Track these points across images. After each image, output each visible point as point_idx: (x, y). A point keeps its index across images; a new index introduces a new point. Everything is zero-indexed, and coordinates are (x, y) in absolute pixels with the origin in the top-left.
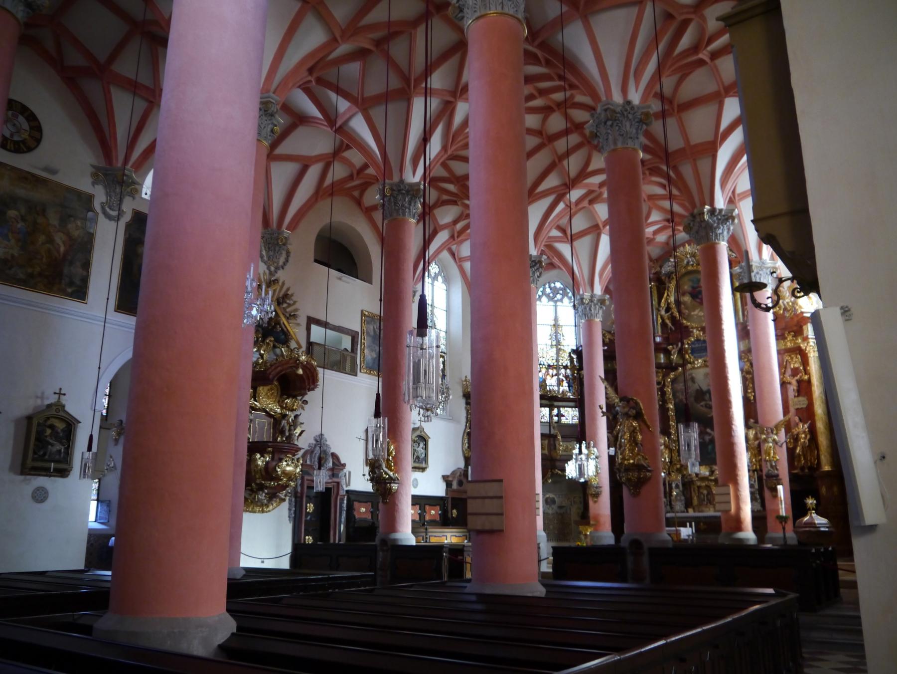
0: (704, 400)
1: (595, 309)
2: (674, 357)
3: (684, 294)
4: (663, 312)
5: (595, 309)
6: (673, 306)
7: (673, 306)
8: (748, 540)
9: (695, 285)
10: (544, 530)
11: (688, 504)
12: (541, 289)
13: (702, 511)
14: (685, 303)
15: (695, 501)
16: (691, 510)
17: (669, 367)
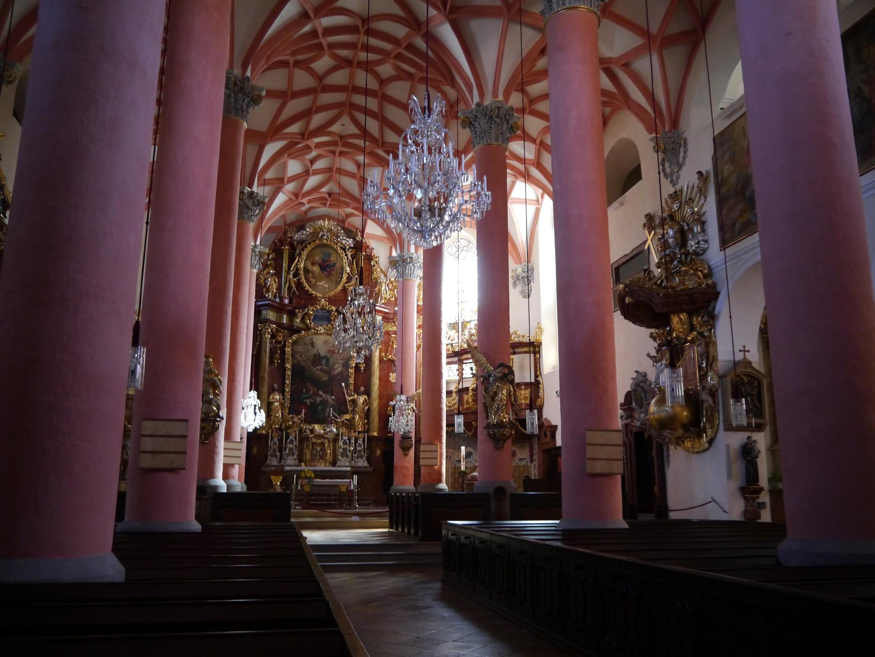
3: (313, 264)
4: (291, 276)
6: (302, 272)
7: (302, 272)
11: (301, 459)
13: (314, 466)
14: (313, 272)
15: (308, 457)
16: (303, 464)
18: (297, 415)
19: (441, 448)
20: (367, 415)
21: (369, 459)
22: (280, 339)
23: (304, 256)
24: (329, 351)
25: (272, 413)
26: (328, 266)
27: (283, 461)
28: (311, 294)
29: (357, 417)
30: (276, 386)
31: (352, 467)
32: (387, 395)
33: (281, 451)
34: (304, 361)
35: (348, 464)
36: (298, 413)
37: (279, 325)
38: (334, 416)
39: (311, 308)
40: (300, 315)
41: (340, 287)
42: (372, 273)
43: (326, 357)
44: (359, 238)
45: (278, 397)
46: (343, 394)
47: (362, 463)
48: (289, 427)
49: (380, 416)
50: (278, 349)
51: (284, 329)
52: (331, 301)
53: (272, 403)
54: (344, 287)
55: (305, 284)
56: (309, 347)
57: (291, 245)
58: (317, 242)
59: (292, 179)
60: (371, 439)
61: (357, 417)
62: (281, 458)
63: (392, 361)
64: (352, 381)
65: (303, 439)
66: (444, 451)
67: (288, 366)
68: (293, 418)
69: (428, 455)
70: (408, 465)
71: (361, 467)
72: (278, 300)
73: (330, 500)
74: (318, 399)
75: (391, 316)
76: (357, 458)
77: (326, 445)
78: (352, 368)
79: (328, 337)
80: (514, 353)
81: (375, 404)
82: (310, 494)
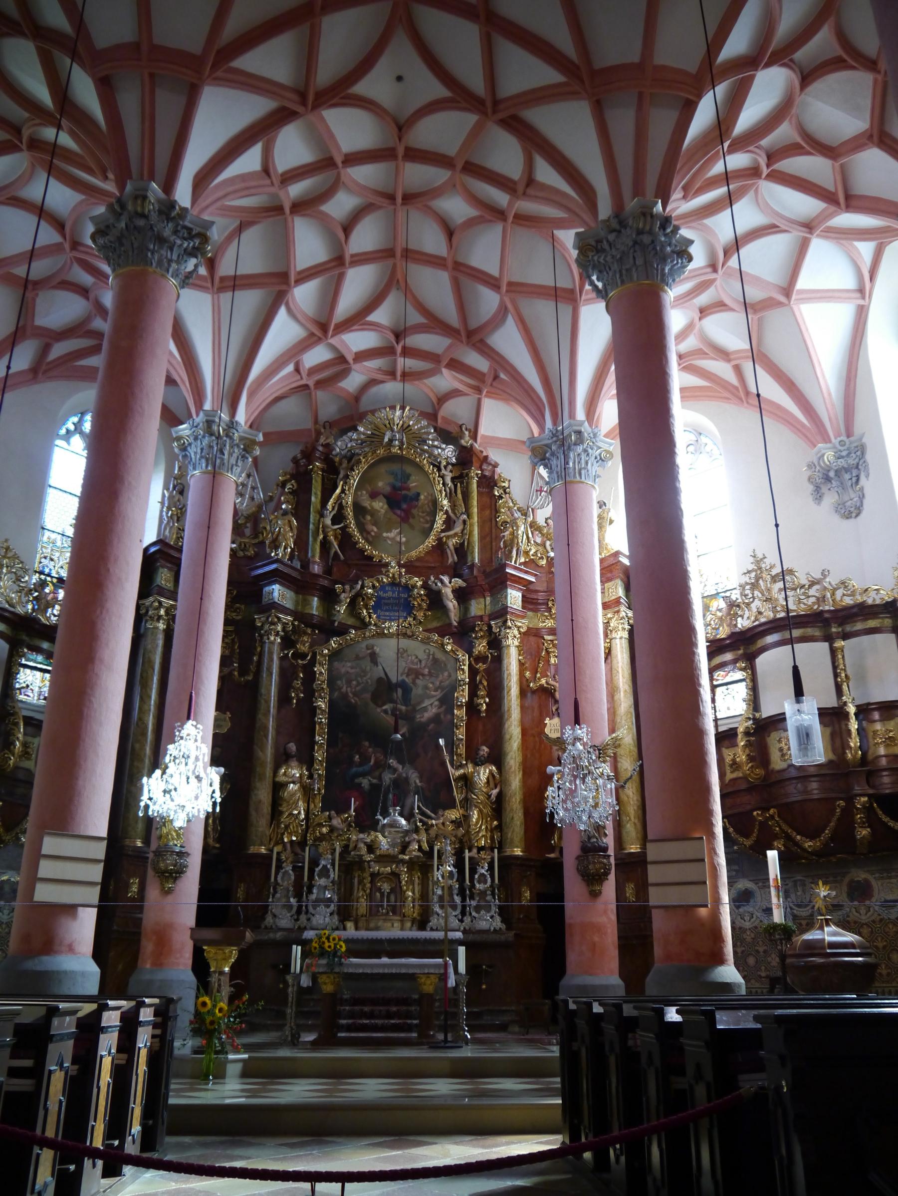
0: (392, 701)
1: (231, 454)
3: (373, 496)
4: (328, 521)
5: (231, 454)
6: (350, 513)
7: (350, 513)
8: (606, 987)
9: (398, 484)
10: (98, 955)
11: (344, 914)
12: (75, 419)
13: (377, 928)
14: (373, 513)
16: (350, 925)
17: (328, 629)
18: (339, 813)
19: (713, 851)
20: (498, 807)
21: (503, 912)
22: (303, 648)
23: (354, 481)
25: (283, 808)
26: (405, 498)
27: (303, 917)
28: (370, 558)
29: (475, 815)
30: (292, 747)
31: (464, 932)
32: (542, 755)
33: (298, 895)
34: (355, 694)
35: (455, 923)
38: (422, 813)
39: (368, 582)
40: (345, 598)
41: (431, 541)
42: (497, 511)
43: (402, 685)
44: (466, 441)
47: (489, 921)
48: (322, 838)
49: (526, 813)
52: (411, 568)
53: (284, 785)
54: (439, 540)
56: (367, 664)
57: (328, 459)
58: (381, 452)
59: (306, 276)
60: (507, 863)
61: (475, 815)
62: (299, 912)
63: (547, 693)
65: (350, 866)
66: (722, 860)
67: (322, 704)
68: (330, 818)
70: (603, 919)
71: (487, 931)
73: (409, 1015)
74: (388, 777)
75: (541, 596)
76: (478, 909)
77: (404, 877)
78: (460, 707)
79: (404, 643)
80: (846, 636)
81: (515, 782)
82: (334, 999)
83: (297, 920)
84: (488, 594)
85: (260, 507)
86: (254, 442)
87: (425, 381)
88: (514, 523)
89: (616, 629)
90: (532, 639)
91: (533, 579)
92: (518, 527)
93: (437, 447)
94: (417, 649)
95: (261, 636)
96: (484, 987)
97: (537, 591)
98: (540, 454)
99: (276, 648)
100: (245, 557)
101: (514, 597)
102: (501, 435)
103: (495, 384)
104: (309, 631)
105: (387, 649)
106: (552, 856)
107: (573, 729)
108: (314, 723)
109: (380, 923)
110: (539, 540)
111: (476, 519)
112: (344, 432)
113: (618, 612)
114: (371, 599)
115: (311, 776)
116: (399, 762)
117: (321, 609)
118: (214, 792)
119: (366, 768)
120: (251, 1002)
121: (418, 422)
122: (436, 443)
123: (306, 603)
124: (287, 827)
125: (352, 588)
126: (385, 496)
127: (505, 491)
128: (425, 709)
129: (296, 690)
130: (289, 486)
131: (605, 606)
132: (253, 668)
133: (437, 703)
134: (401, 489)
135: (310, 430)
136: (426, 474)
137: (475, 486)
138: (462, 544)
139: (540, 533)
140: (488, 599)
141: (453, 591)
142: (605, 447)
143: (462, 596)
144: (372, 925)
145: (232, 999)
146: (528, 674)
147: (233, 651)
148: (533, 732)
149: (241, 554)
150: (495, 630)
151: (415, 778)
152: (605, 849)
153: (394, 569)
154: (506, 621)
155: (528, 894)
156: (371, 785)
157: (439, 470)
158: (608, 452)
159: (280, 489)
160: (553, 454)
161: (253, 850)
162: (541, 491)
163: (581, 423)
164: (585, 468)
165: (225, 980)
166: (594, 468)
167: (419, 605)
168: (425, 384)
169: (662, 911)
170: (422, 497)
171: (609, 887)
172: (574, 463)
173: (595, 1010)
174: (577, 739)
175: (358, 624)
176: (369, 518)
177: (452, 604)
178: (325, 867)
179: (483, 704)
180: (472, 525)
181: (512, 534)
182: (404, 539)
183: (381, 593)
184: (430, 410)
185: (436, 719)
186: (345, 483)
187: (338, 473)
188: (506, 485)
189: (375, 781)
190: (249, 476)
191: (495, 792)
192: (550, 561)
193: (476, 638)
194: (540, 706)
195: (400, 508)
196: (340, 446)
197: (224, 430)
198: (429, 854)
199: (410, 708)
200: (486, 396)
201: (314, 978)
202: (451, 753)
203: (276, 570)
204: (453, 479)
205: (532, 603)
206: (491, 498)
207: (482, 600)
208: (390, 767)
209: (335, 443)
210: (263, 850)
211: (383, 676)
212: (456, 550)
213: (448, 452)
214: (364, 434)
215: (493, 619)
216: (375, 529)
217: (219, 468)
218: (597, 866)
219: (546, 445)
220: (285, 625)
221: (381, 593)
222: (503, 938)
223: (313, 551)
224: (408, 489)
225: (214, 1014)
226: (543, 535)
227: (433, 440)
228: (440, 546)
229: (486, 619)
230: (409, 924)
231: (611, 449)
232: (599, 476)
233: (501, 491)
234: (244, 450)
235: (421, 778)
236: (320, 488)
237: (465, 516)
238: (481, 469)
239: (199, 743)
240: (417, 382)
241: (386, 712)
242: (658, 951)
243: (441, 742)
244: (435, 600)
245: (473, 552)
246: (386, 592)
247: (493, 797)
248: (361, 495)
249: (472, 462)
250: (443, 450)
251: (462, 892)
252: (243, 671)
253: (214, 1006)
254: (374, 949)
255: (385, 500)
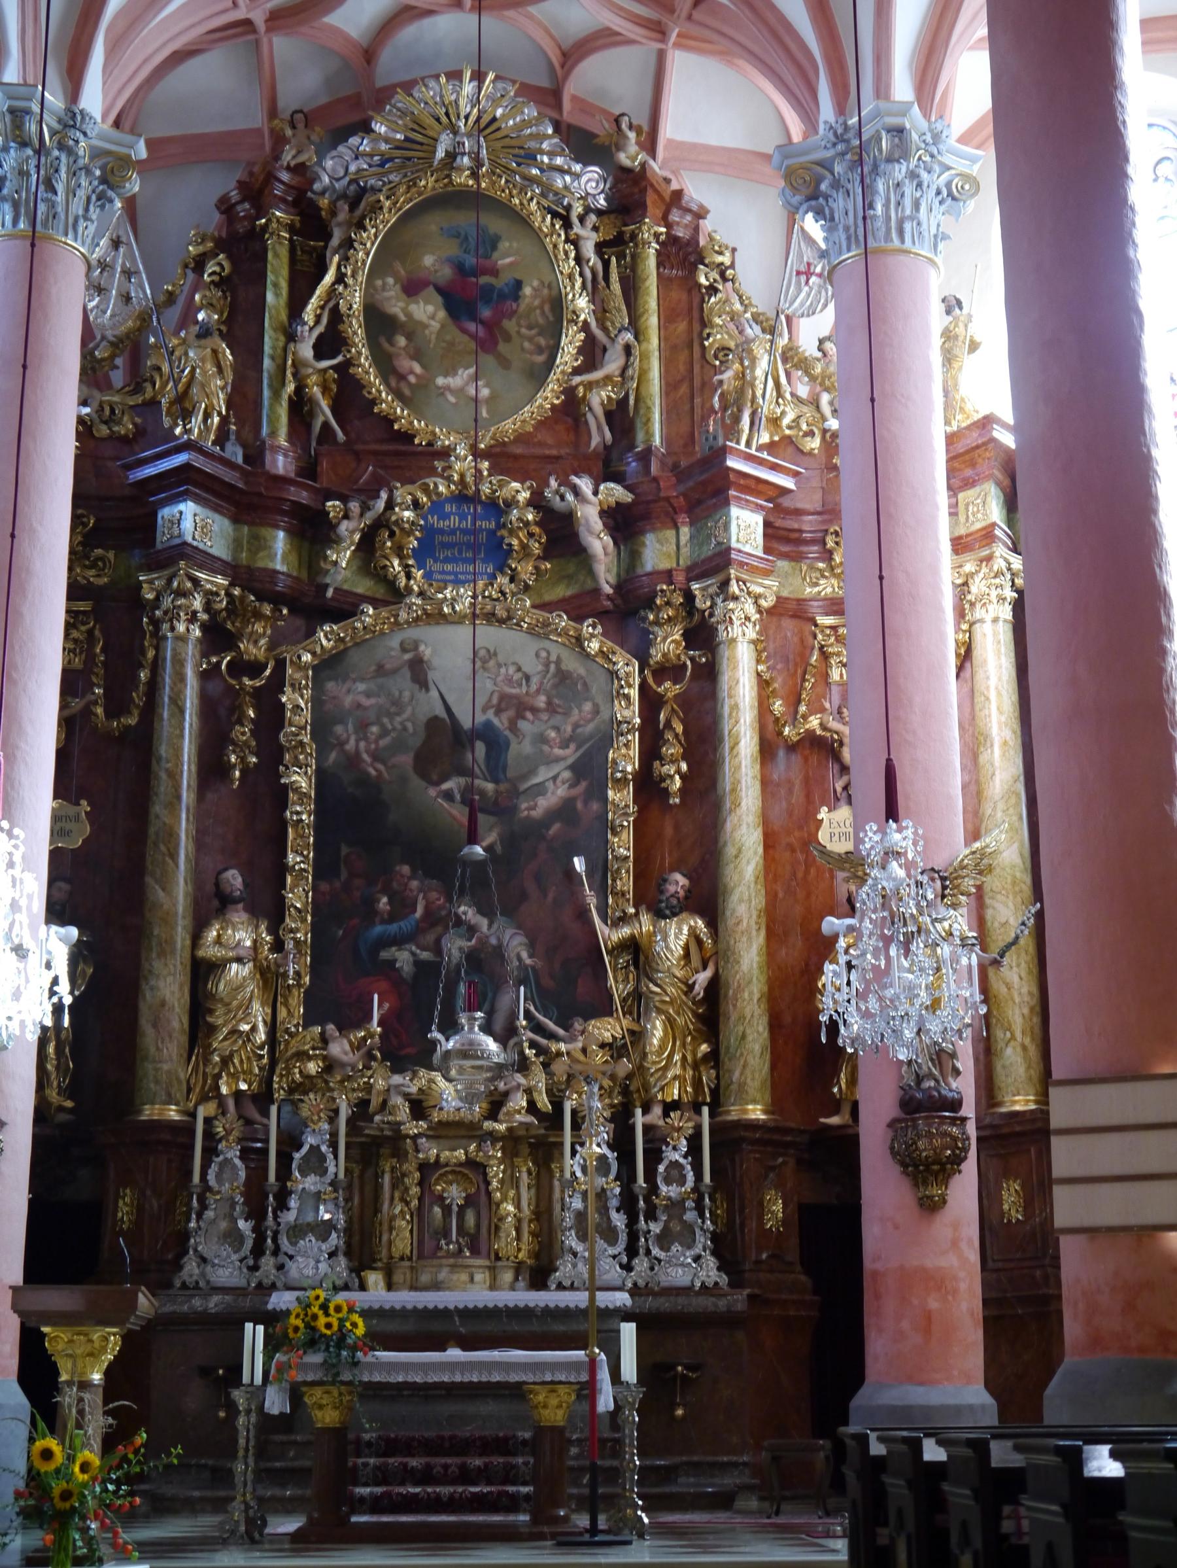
0: (462, 771)
1: (71, 192)
2: (343, 557)
3: (412, 289)
4: (306, 350)
5: (71, 192)
7: (356, 330)
9: (470, 261)
11: (362, 1250)
13: (436, 1286)
14: (412, 330)
15: (402, 1239)
16: (374, 1278)
17: (313, 605)
20: (711, 1012)
22: (254, 649)
24: (504, 703)
26: (487, 294)
28: (407, 437)
29: (657, 1031)
30: (234, 879)
31: (635, 1291)
32: (810, 894)
33: (256, 1213)
35: (611, 1271)
36: (350, 1017)
37: (244, 575)
38: (538, 1028)
39: (403, 494)
40: (350, 531)
41: (549, 396)
43: (487, 734)
44: (630, 155)
45: (243, 937)
46: (582, 914)
47: (690, 1267)
48: (307, 1085)
49: (775, 1025)
50: (243, 703)
51: (277, 600)
52: (503, 458)
55: (387, 402)
56: (403, 685)
58: (428, 183)
60: (730, 1138)
62: (258, 1250)
63: (824, 748)
64: (623, 845)
65: (372, 1146)
67: (301, 780)
68: (324, 1040)
69: (1108, 1155)
70: (949, 1261)
71: (687, 1290)
72: (235, 453)
73: (510, 1476)
74: (455, 947)
75: (809, 524)
76: (664, 1240)
77: (496, 1172)
78: (621, 783)
79: (489, 635)
81: (749, 956)
82: (340, 1440)
83: (255, 1268)
84: (683, 518)
85: (144, 319)
86: (125, 162)
87: (532, 9)
88: (745, 350)
89: (983, 599)
90: (788, 624)
91: (788, 483)
92: (753, 360)
93: (561, 171)
94: (520, 651)
95: (156, 623)
96: (680, 1412)
97: (798, 512)
98: (807, 186)
99: (191, 651)
100: (114, 438)
101: (745, 526)
102: (713, 142)
103: (697, 15)
104: (267, 609)
105: (449, 650)
106: (835, 1120)
107: (882, 831)
108: (283, 825)
109: (443, 1275)
110: (803, 391)
111: (655, 341)
112: (340, 136)
113: (989, 559)
114: (409, 533)
115: (278, 946)
116: (481, 912)
117: (293, 558)
118: (55, 981)
119: (405, 925)
120: (154, 1448)
121: (515, 109)
122: (559, 161)
123: (259, 545)
124: (226, 1061)
125: (365, 508)
126: (439, 290)
127: (722, 275)
128: (540, 789)
129: (240, 747)
130: (211, 267)
131: (960, 545)
132: (138, 698)
133: (567, 775)
134: (478, 271)
135: (258, 131)
136: (536, 235)
137: (651, 262)
138: (623, 403)
139: (807, 373)
140: (685, 531)
141: (603, 514)
142: (960, 165)
143: (624, 524)
144: (425, 1278)
145: (109, 1443)
146: (778, 706)
147: (90, 659)
148: (789, 842)
149: (104, 431)
150: (702, 603)
151: (517, 948)
152: (955, 1104)
153: (463, 463)
154: (726, 583)
155: (778, 1207)
156: (418, 963)
157: (567, 225)
158: (966, 177)
159: (191, 275)
160: (836, 185)
161: (149, 1112)
162: (809, 274)
163: (904, 110)
164: (912, 218)
165: (93, 1399)
166: (933, 217)
167: (524, 547)
168: (531, 17)
169: (1081, 1238)
170: (527, 291)
171: (964, 1190)
172: (887, 205)
173: (928, 1456)
174: (891, 854)
175: (380, 592)
176: (402, 341)
177: (599, 544)
178: (315, 1149)
179: (674, 774)
180: (644, 357)
181: (741, 376)
182: (485, 392)
183: (433, 520)
184: (544, 83)
185: (565, 812)
186: (346, 259)
187: (328, 236)
188: (726, 259)
189: (425, 955)
190: (116, 244)
191: (703, 978)
192: (831, 441)
193: (657, 623)
194: (806, 781)
195: (474, 317)
196: (334, 169)
197: (53, 133)
198: (554, 1119)
199: (503, 787)
200: (677, 45)
201: (296, 1394)
202: (602, 890)
203: (187, 467)
204: (600, 247)
205: (788, 541)
206: (690, 291)
207: (670, 534)
208: (459, 922)
209: (319, 163)
210: (173, 1114)
211: (440, 711)
212: (609, 415)
213: (589, 183)
214: (387, 140)
215: (697, 578)
216: (418, 369)
217: (45, 224)
218: (937, 1142)
219: (820, 163)
220: (210, 597)
221: (433, 520)
222: (722, 1304)
223: (273, 422)
224: (494, 272)
225: (69, 1477)
226: (813, 379)
227: (551, 154)
228: (571, 408)
229: (680, 578)
230: (508, 1277)
231: (975, 170)
232: (945, 237)
233: (715, 275)
234: (103, 180)
235: (532, 946)
236: (285, 272)
237: (629, 337)
238: (665, 220)
239: (17, 872)
240: (510, 13)
241: (448, 796)
242: (1072, 1329)
243: (579, 864)
244: (561, 534)
245: (648, 421)
246: (444, 517)
247: (699, 990)
248: (384, 288)
249: (644, 206)
250: (577, 176)
251: (628, 1204)
252: (116, 705)
253: (71, 1459)
254: (430, 1330)
255: (439, 299)
